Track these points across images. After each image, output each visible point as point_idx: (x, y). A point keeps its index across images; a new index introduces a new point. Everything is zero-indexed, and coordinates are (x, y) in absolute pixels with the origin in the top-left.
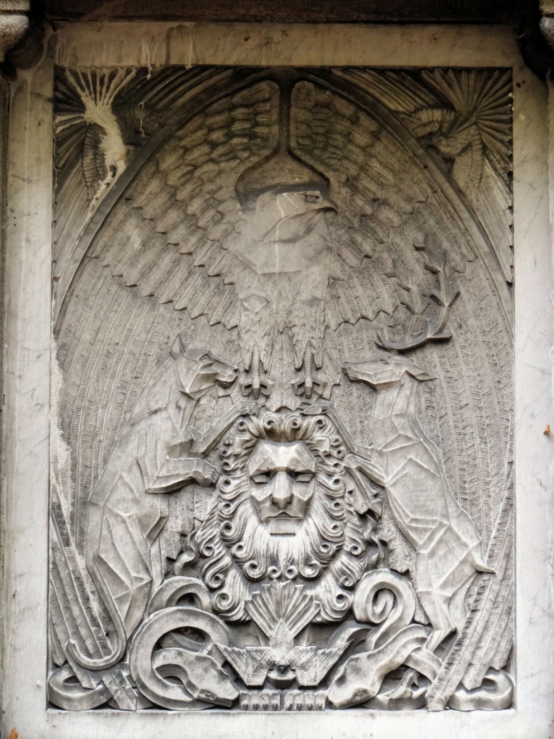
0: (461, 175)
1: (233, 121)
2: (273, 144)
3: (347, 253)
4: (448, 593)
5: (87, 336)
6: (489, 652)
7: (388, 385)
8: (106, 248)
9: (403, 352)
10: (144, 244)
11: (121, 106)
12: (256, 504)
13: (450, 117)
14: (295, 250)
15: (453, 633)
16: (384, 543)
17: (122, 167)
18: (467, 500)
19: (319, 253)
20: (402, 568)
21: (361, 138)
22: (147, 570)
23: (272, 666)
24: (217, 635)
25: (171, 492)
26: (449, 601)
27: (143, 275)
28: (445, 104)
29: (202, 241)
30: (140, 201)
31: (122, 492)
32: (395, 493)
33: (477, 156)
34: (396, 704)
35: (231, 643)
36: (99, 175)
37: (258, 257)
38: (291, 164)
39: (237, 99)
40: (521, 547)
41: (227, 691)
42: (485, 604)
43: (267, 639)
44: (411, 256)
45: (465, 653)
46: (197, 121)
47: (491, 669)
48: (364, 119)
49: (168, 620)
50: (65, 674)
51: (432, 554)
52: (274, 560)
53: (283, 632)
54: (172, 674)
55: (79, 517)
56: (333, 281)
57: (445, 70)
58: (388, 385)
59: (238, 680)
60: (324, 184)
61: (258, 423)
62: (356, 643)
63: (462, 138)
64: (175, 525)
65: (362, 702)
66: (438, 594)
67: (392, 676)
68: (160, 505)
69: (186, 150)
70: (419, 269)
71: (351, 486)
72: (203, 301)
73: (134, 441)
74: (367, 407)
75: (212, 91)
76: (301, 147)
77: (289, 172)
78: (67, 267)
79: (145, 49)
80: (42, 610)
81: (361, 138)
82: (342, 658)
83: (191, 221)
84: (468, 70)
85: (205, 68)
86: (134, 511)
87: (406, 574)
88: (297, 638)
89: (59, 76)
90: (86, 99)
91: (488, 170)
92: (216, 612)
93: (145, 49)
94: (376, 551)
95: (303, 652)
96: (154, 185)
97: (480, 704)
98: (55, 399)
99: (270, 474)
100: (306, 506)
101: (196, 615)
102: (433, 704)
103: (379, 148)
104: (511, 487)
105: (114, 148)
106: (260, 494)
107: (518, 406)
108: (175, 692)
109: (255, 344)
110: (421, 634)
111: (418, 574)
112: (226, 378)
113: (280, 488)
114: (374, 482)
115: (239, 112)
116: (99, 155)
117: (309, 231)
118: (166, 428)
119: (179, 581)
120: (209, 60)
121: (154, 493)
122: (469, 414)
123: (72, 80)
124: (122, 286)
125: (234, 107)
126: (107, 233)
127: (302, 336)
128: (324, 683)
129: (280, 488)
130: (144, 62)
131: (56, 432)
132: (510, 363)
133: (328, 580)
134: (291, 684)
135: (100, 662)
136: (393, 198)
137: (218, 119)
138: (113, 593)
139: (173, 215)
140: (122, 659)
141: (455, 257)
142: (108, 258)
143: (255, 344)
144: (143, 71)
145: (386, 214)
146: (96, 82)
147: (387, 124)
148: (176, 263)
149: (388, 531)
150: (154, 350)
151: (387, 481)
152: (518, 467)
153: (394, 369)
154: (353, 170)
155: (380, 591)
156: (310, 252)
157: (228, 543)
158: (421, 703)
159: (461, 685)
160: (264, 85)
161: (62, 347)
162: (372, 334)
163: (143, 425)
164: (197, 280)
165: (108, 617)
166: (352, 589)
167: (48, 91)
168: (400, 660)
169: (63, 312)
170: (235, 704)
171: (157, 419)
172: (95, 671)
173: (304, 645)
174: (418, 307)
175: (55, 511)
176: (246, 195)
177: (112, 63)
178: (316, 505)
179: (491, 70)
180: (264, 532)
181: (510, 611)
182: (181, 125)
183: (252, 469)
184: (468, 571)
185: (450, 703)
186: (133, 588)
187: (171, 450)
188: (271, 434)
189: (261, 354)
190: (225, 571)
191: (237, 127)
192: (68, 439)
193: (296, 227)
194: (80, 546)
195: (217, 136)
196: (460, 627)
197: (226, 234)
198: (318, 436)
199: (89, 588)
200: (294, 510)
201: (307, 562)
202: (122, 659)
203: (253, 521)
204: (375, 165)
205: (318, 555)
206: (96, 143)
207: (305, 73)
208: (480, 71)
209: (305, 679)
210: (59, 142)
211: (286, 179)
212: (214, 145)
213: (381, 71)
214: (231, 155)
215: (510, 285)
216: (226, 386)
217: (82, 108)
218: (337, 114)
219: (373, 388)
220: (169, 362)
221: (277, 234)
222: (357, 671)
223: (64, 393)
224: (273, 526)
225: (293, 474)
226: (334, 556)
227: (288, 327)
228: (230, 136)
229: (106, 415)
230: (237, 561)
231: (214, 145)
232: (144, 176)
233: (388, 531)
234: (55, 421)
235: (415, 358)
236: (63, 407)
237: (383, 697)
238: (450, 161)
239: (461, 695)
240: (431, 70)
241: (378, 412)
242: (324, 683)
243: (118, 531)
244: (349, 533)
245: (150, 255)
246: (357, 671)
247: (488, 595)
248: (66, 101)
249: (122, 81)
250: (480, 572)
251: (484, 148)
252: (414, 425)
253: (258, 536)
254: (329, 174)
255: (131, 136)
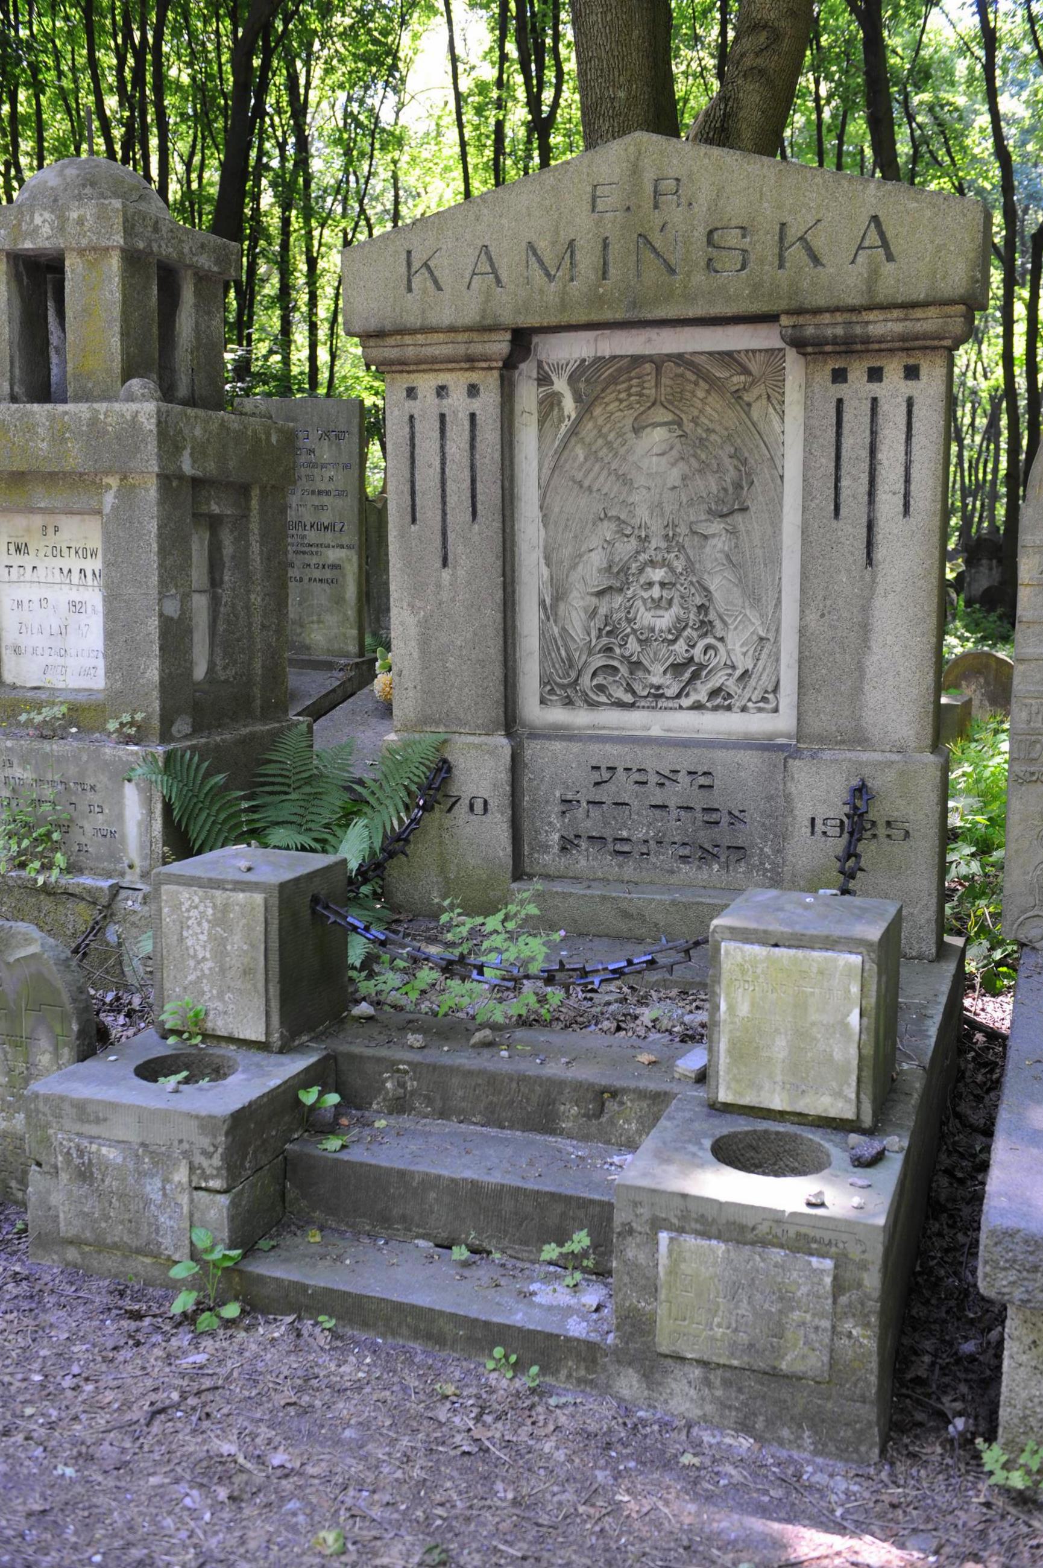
0: (755, 414)
1: (631, 387)
2: (652, 399)
3: (692, 460)
4: (744, 649)
5: (557, 510)
6: (766, 682)
7: (713, 536)
8: (566, 461)
9: (722, 516)
10: (586, 459)
11: (572, 380)
12: (644, 601)
13: (750, 379)
14: (664, 460)
15: (747, 671)
16: (710, 622)
17: (573, 416)
18: (754, 599)
19: (677, 461)
20: (719, 635)
21: (700, 394)
22: (589, 634)
23: (652, 686)
24: (624, 670)
25: (600, 594)
26: (745, 654)
27: (586, 476)
28: (746, 371)
29: (616, 455)
30: (583, 434)
31: (575, 593)
32: (717, 595)
33: (764, 401)
34: (716, 708)
35: (631, 673)
36: (561, 420)
37: (644, 464)
38: (662, 410)
39: (633, 374)
40: (784, 625)
41: (628, 698)
42: (764, 656)
43: (649, 672)
44: (727, 461)
45: (753, 682)
46: (612, 387)
47: (766, 692)
48: (702, 383)
49: (599, 661)
50: (548, 687)
51: (736, 628)
52: (653, 630)
53: (658, 669)
54: (601, 688)
55: (555, 606)
56: (684, 478)
57: (747, 351)
58: (713, 536)
59: (634, 693)
60: (680, 424)
61: (643, 557)
62: (695, 676)
63: (756, 392)
64: (603, 611)
65: (697, 707)
66: (738, 650)
67: (714, 693)
68: (594, 600)
69: (607, 404)
70: (731, 468)
71: (693, 591)
72: (615, 489)
73: (580, 567)
74: (702, 547)
75: (619, 370)
76: (668, 401)
77: (661, 415)
78: (546, 472)
79: (585, 349)
80: (537, 654)
81: (700, 394)
82: (688, 683)
83: (609, 444)
84: (760, 351)
85: (615, 357)
86: (581, 603)
87: (721, 639)
88: (665, 672)
89: (540, 365)
90: (554, 378)
91: (771, 410)
92: (623, 656)
93: (585, 349)
94: (705, 627)
95: (668, 679)
96: (590, 425)
97: (760, 710)
98: (541, 544)
99: (650, 584)
100: (670, 602)
101: (613, 658)
102: (735, 709)
103: (710, 399)
104: (780, 592)
105: (569, 405)
106: (646, 595)
107: (784, 547)
108: (603, 699)
109: (643, 514)
110: (730, 671)
111: (729, 640)
112: (628, 532)
113: (656, 592)
114: (706, 589)
115: (634, 382)
116: (561, 409)
117: (671, 448)
118: (597, 559)
119: (605, 640)
120: (618, 353)
121: (592, 594)
122: (759, 552)
123: (547, 368)
124: (574, 482)
125: (631, 379)
126: (566, 452)
127: (668, 509)
128: (678, 696)
129: (656, 592)
130: (584, 355)
131: (542, 561)
132: (781, 521)
133: (681, 641)
134: (662, 695)
135: (566, 681)
136: (718, 428)
137: (624, 386)
138: (573, 646)
139: (600, 441)
140: (577, 680)
141: (751, 461)
142: (567, 466)
143: (643, 514)
144: (584, 360)
145: (713, 437)
146: (559, 368)
147: (714, 384)
148: (602, 469)
149: (712, 616)
150: (591, 517)
151: (712, 588)
152: (784, 581)
153: (716, 527)
154: (696, 413)
155: (707, 648)
156: (672, 460)
157: (629, 621)
158: (729, 708)
159: (750, 700)
160: (647, 365)
161: (544, 516)
162: (706, 506)
163: (585, 558)
164: (613, 478)
165: (570, 660)
166: (693, 647)
167: (534, 375)
168: (718, 685)
169: (544, 497)
170: (632, 706)
171: (592, 554)
172: (563, 687)
173: (668, 676)
174: (731, 490)
175: (542, 603)
176: (637, 430)
177: (567, 356)
178: (675, 601)
179: (773, 350)
180: (648, 615)
181: (778, 660)
182: (603, 390)
183: (642, 581)
184: (755, 638)
185: (744, 709)
186: (581, 644)
187: (600, 571)
188: (652, 563)
189: (646, 518)
190: (627, 636)
191: (634, 390)
192: (548, 565)
193: (664, 447)
194: (555, 621)
195: (623, 396)
196: (750, 668)
197: (628, 451)
198: (675, 563)
199: (560, 643)
200: (664, 603)
201: (670, 631)
202: (577, 680)
203: (642, 609)
204: (708, 408)
205: (675, 628)
206: (559, 403)
207: (670, 357)
208: (766, 351)
209: (669, 693)
210: (541, 403)
211: (660, 419)
212: (621, 401)
213: (710, 354)
214: (630, 407)
215: (782, 477)
216: (628, 536)
217: (552, 383)
218: (687, 380)
219: (706, 537)
220: (599, 523)
221: (655, 451)
222: (695, 690)
223: (546, 541)
224: (652, 612)
225: (663, 585)
226: (684, 628)
227: (660, 504)
228: (630, 395)
229: (567, 552)
230: (634, 631)
231: (621, 401)
232: (585, 420)
233: (712, 616)
234: (541, 556)
235: (729, 520)
236: (545, 548)
237: (709, 705)
238: (749, 405)
239: (750, 704)
240: (739, 352)
241: (708, 550)
242: (678, 696)
243: (574, 614)
244: (692, 616)
245: (588, 464)
246: (695, 690)
247: (765, 651)
248: (544, 380)
249: (570, 369)
250: (761, 639)
251: (769, 397)
252: (727, 556)
253: (645, 617)
254: (683, 416)
255: (578, 398)
